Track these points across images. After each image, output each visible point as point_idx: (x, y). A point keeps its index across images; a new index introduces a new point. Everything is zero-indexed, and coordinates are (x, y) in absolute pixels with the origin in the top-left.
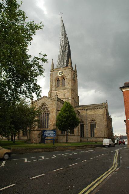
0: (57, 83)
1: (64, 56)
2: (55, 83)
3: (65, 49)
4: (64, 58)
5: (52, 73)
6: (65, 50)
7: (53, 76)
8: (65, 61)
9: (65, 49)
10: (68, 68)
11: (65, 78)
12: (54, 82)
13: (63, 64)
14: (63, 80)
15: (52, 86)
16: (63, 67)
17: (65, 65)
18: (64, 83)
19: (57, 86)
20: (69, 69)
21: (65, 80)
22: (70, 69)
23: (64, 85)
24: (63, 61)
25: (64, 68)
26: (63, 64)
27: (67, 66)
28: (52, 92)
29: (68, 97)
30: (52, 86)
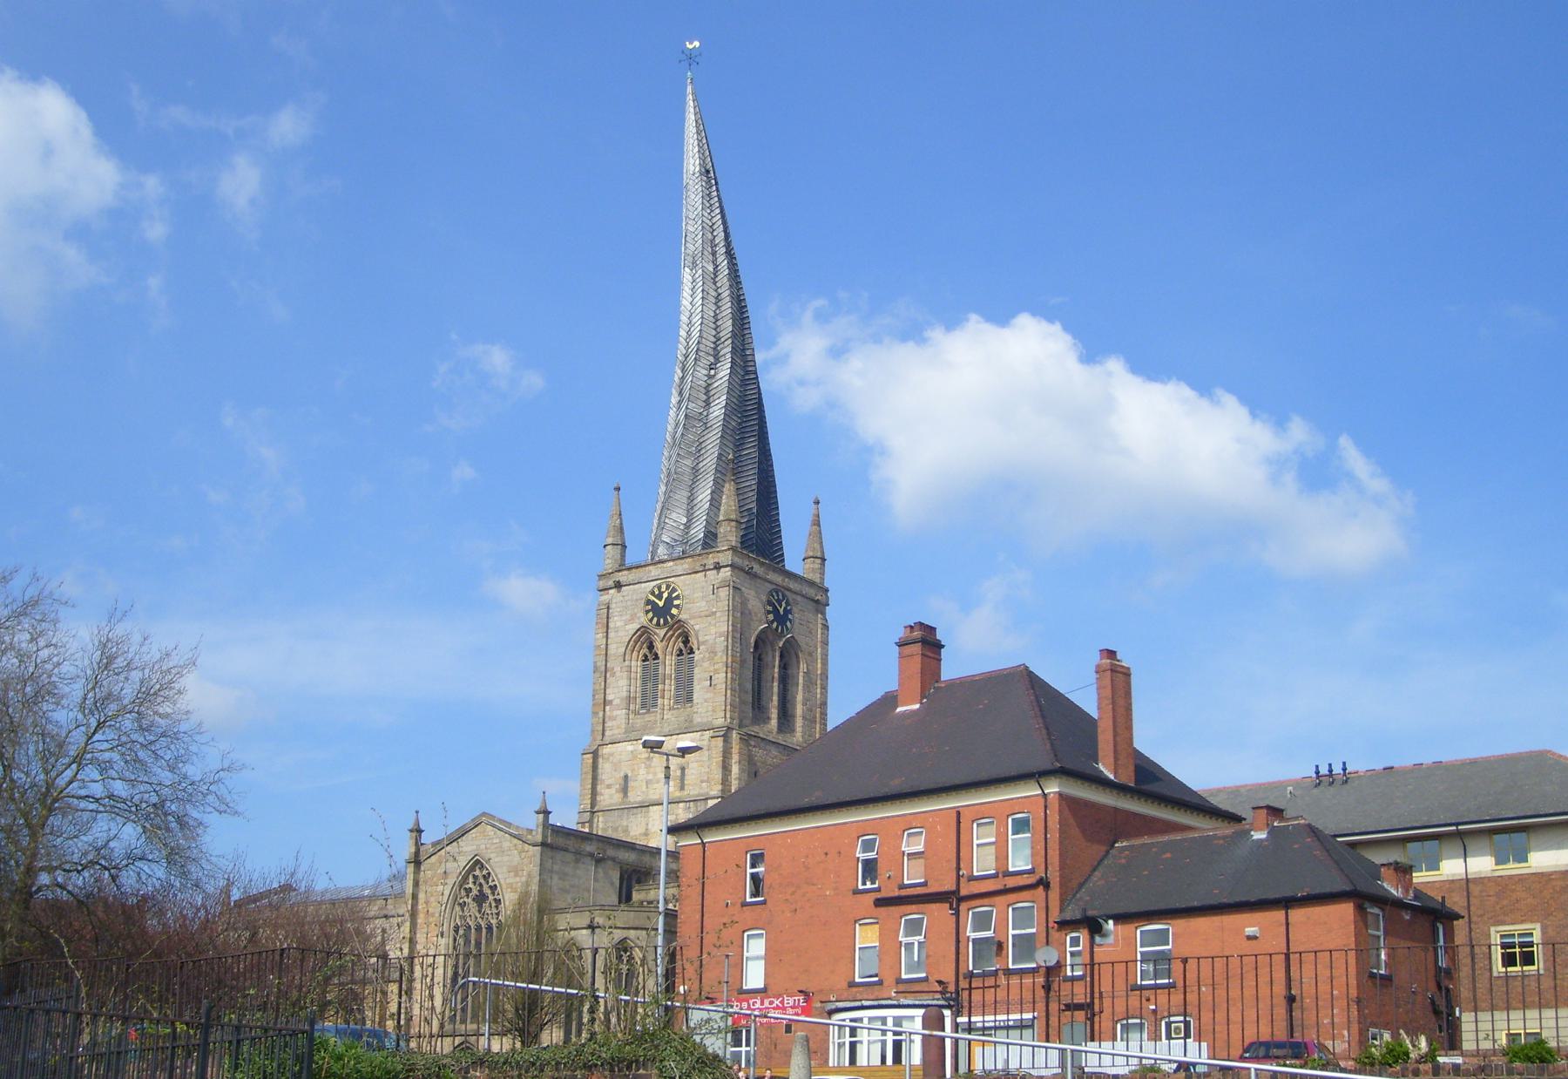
0: (644, 683)
1: (698, 455)
2: (624, 682)
3: (707, 392)
4: (695, 471)
5: (605, 598)
6: (708, 403)
7: (616, 622)
8: (704, 496)
9: (707, 392)
10: (710, 561)
11: (694, 643)
12: (617, 669)
13: (688, 526)
14: (680, 653)
15: (605, 703)
16: (684, 556)
17: (698, 531)
18: (691, 680)
19: (648, 700)
20: (718, 567)
21: (697, 656)
22: (726, 573)
23: (689, 699)
24: (691, 498)
25: (685, 565)
26: (688, 526)
27: (710, 538)
28: (606, 750)
29: (704, 789)
30: (605, 703)
